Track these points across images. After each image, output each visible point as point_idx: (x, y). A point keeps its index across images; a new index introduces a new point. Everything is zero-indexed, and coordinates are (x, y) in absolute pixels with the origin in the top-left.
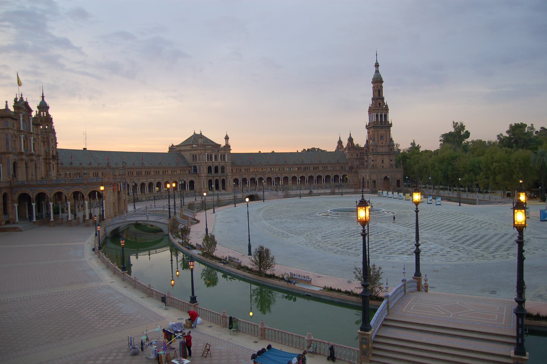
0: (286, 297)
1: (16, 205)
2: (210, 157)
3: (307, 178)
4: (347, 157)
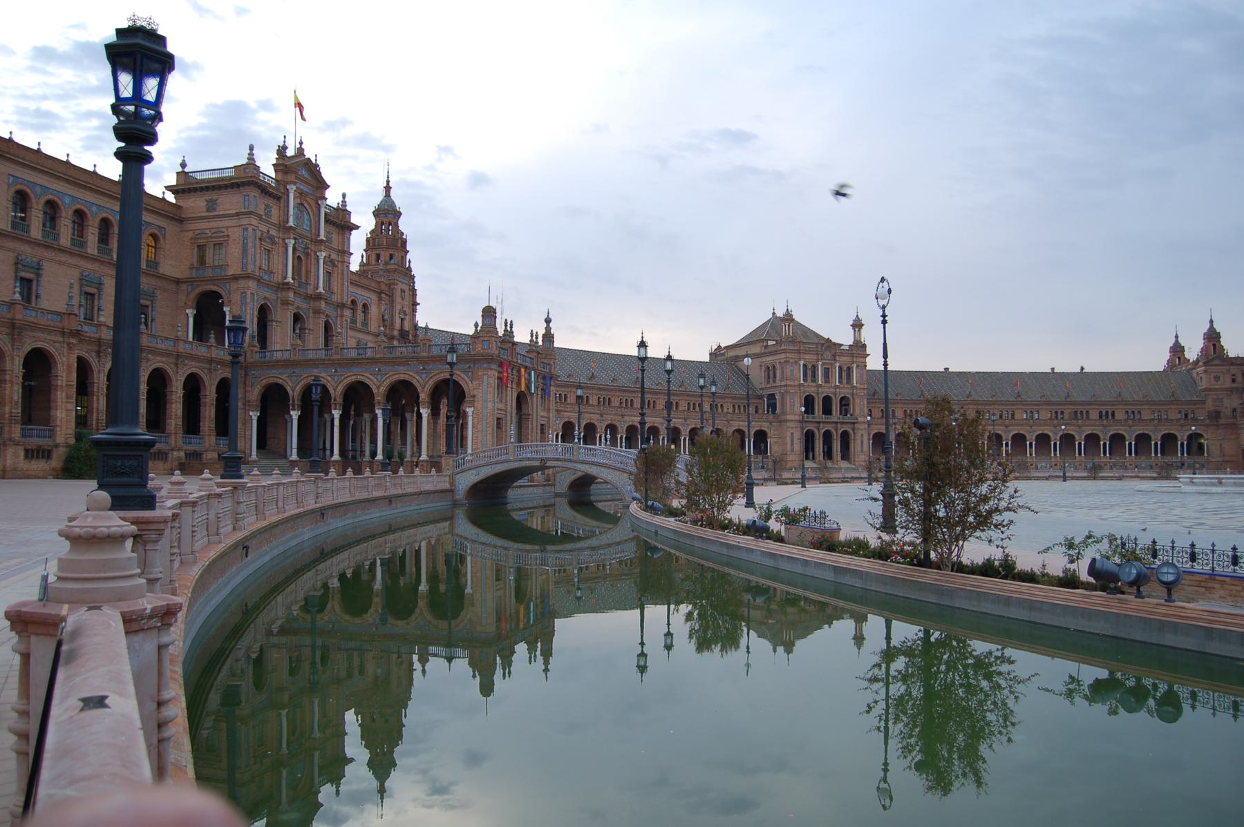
0: (1099, 690)
1: (255, 415)
2: (810, 372)
3: (1080, 439)
4: (1203, 385)
